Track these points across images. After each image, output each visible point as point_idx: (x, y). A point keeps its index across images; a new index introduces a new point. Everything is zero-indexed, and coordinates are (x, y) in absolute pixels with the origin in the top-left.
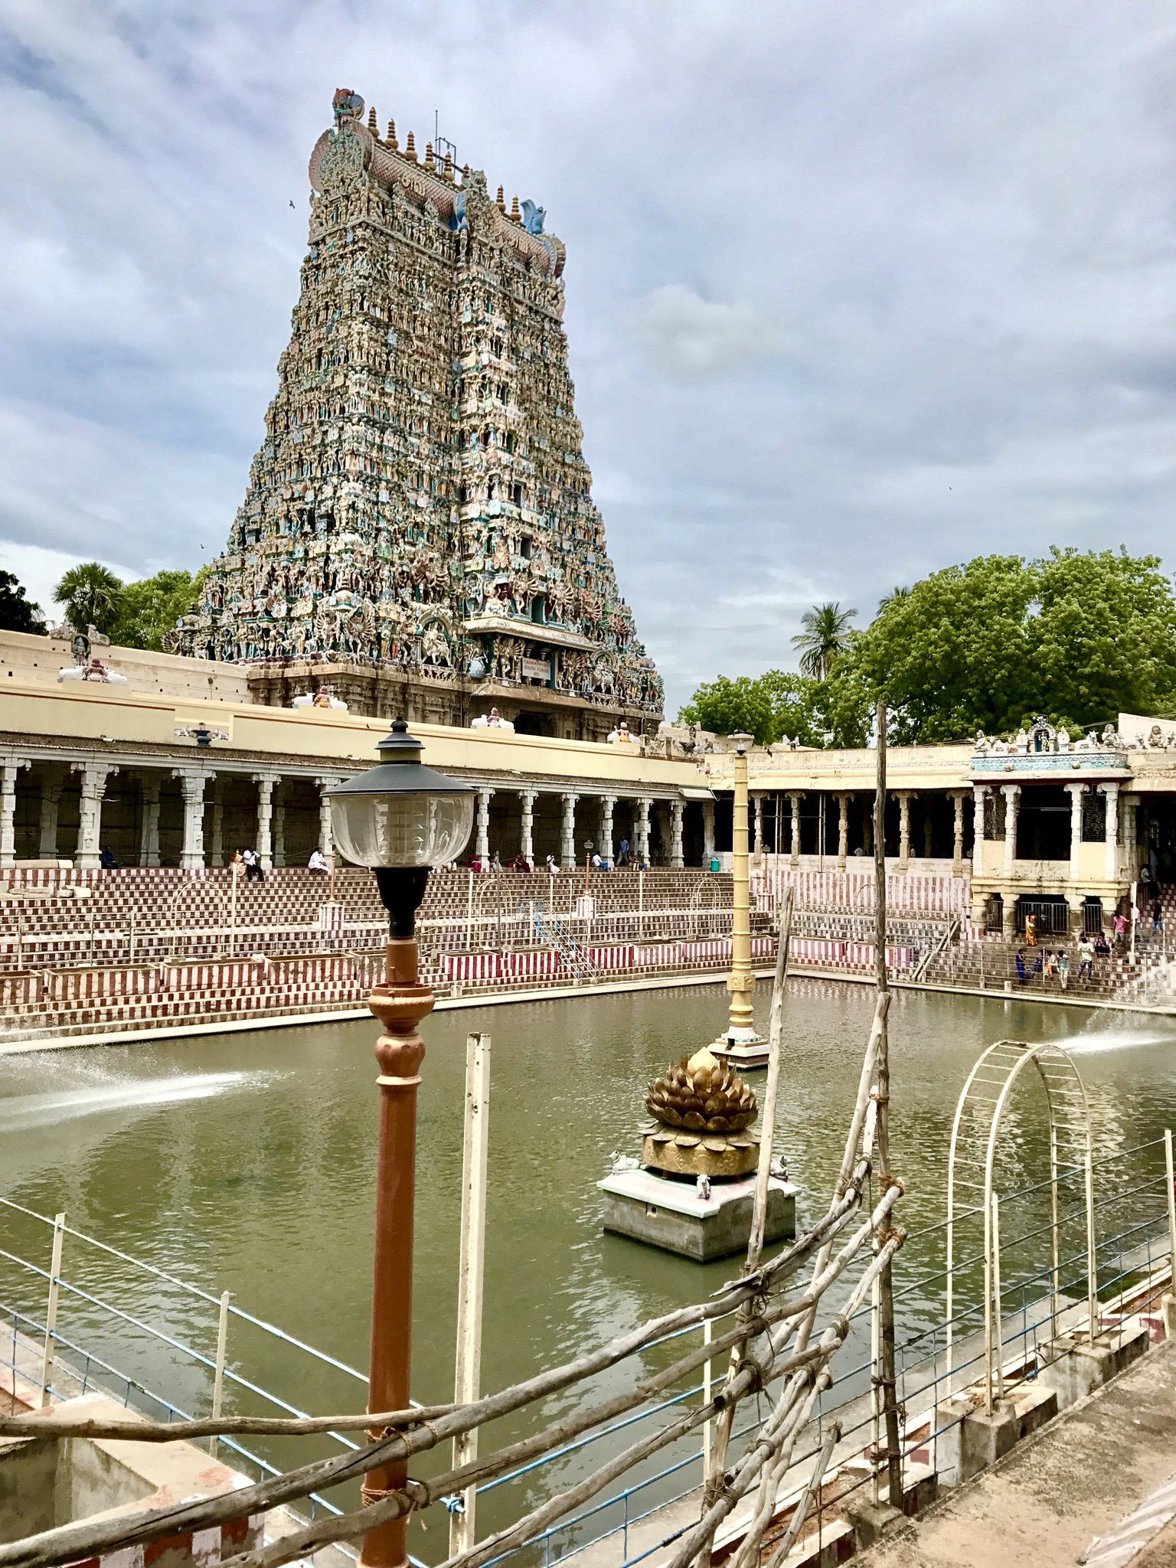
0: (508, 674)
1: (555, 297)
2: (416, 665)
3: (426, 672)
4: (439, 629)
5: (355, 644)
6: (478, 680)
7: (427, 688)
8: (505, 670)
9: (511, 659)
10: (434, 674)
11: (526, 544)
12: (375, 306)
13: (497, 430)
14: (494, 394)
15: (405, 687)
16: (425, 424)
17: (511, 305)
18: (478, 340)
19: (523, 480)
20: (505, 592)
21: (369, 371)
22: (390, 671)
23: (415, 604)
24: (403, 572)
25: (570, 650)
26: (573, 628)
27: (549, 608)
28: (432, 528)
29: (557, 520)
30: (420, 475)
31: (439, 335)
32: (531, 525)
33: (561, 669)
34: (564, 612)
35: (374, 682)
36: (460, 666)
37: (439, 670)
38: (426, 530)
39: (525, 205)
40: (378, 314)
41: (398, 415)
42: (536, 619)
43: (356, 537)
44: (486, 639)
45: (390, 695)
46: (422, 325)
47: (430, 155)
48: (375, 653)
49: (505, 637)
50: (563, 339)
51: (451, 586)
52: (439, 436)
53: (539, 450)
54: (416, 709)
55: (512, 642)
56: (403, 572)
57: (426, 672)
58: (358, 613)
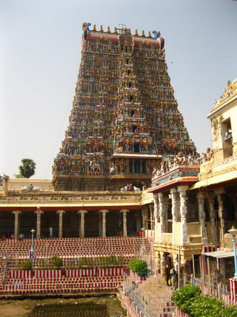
0: (123, 171)
1: (162, 54)
2: (87, 172)
3: (90, 174)
4: (96, 159)
5: (62, 168)
6: (113, 173)
7: (91, 179)
8: (121, 169)
9: (123, 165)
10: (94, 174)
11: (134, 128)
12: (87, 73)
13: (125, 96)
14: (126, 86)
15: (83, 179)
16: (103, 101)
17: (143, 61)
18: (123, 72)
19: (135, 108)
20: (122, 144)
21: (82, 90)
22: (77, 175)
23: (88, 154)
24: (87, 145)
25: (151, 159)
26: (154, 151)
27: (143, 146)
28: (102, 130)
29: (159, 119)
30: (99, 115)
31: (112, 75)
32: (137, 122)
33: (148, 166)
34: (149, 147)
35: (69, 179)
36: (107, 170)
37: (95, 173)
38: (99, 131)
39: (153, 32)
40: (88, 74)
41: (93, 100)
42: (137, 151)
43: (70, 137)
44: (115, 159)
45: (76, 183)
46: (104, 74)
47: (116, 29)
48: (71, 170)
49: (120, 158)
50: (166, 64)
51: (108, 146)
52: (110, 103)
53: (152, 99)
54: (89, 186)
55: (122, 160)
56: (87, 145)
57: (90, 174)
58: (62, 159)
